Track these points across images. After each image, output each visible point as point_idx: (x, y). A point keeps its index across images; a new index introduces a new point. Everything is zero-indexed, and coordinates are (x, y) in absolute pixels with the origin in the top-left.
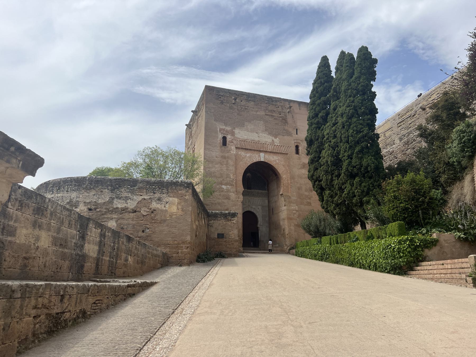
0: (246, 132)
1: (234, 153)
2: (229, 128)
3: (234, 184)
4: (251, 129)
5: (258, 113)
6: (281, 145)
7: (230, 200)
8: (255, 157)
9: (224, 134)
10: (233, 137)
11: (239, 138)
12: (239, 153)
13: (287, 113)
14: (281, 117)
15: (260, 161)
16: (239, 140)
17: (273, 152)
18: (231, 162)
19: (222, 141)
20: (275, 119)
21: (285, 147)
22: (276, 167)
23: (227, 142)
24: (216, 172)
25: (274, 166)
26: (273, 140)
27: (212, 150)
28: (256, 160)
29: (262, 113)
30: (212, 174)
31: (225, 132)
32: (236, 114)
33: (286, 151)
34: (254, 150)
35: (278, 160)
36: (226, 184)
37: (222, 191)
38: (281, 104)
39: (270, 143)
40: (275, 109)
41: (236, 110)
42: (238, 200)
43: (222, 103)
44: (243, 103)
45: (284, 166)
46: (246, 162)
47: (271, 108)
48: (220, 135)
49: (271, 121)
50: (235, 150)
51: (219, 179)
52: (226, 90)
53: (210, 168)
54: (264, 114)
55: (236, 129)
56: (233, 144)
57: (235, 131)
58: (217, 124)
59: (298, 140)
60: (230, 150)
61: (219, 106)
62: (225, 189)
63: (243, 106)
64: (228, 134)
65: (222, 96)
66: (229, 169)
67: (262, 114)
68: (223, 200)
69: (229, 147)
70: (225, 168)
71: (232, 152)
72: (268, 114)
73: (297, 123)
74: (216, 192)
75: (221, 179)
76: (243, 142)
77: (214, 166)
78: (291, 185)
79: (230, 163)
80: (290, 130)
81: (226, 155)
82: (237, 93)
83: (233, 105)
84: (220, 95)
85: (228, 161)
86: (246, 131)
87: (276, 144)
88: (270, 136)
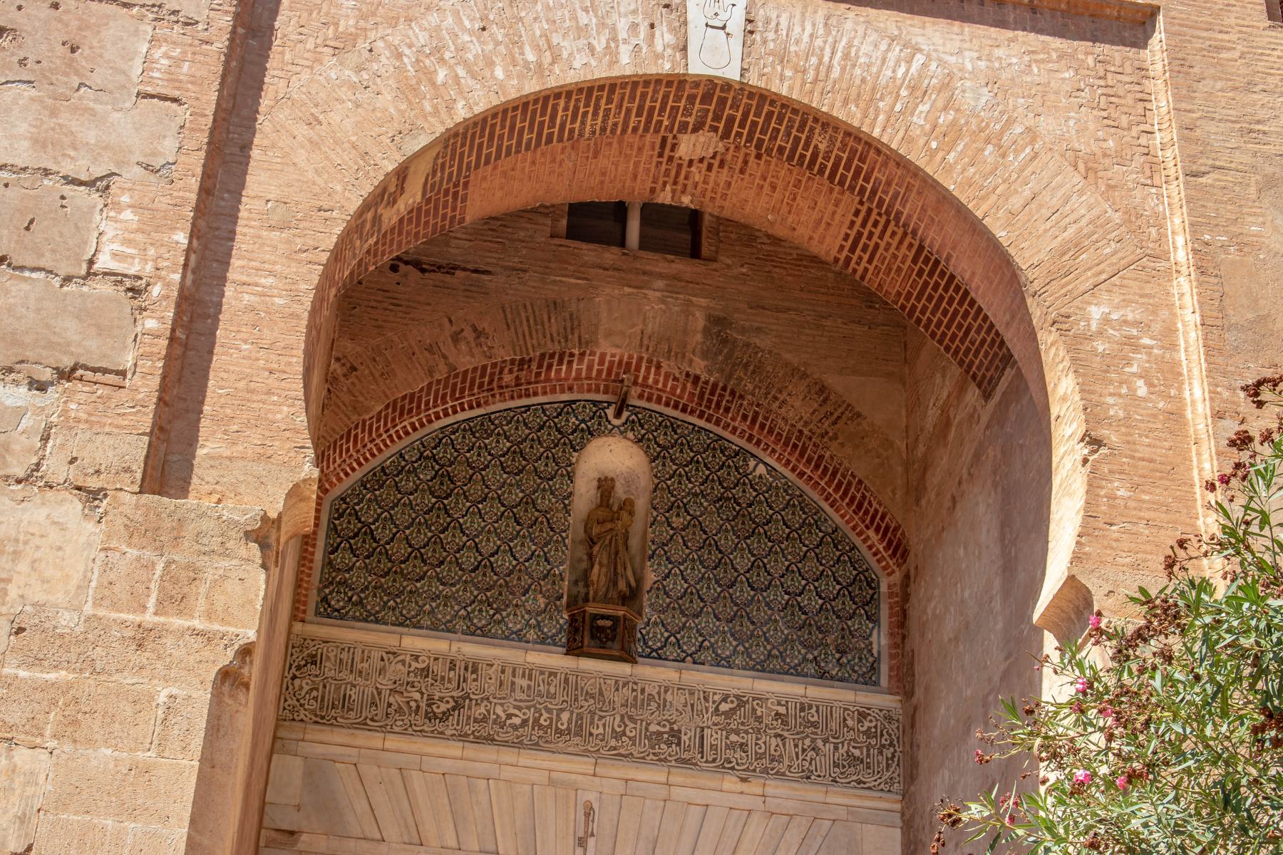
15: (666, 67)
25: (917, 157)
42: (143, 638)
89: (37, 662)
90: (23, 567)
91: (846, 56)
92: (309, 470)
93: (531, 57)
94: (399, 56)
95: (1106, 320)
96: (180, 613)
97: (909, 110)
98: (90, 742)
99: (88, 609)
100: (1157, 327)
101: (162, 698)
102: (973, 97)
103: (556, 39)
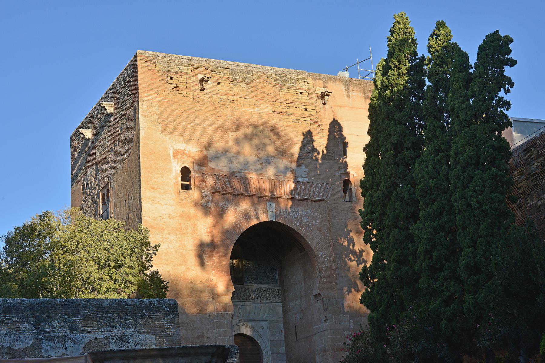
5: (257, 110)
25: (298, 231)
27: (160, 202)
32: (208, 114)
33: (323, 195)
35: (306, 216)
41: (208, 104)
44: (224, 87)
45: (319, 229)
58: (167, 138)
63: (222, 94)
65: (176, 73)
67: (266, 111)
77: (167, 238)
84: (170, 72)
85: (195, 225)
91: (288, 214)
97: (297, 223)
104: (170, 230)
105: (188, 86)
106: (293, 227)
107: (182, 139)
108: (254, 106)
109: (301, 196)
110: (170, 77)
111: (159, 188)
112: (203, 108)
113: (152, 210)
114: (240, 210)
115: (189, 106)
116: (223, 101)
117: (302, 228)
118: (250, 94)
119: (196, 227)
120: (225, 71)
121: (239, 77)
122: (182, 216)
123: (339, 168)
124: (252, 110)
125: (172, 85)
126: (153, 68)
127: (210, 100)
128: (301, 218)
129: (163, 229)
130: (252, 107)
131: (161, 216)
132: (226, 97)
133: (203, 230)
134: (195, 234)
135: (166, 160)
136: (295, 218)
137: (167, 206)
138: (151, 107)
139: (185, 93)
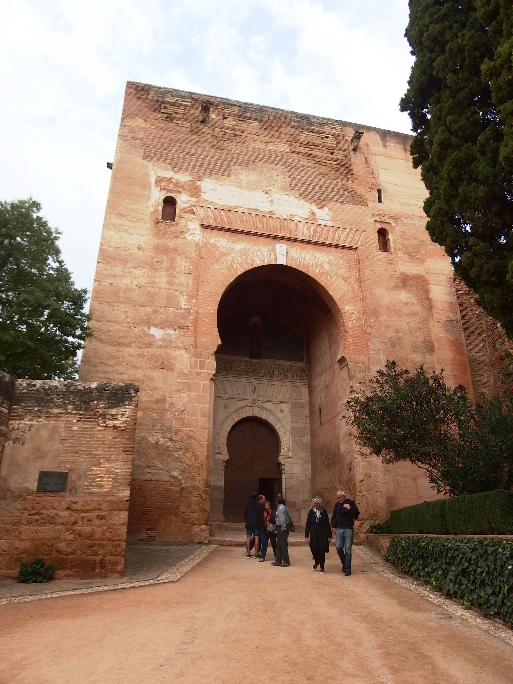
0: (234, 188)
1: (197, 238)
2: (184, 178)
3: (189, 324)
4: (250, 182)
5: (271, 147)
6: (336, 226)
7: (172, 370)
8: (259, 254)
9: (168, 191)
10: (195, 199)
11: (215, 203)
12: (212, 241)
13: (352, 152)
14: (334, 160)
15: (273, 263)
16: (212, 207)
17: (313, 243)
18: (182, 264)
19: (160, 208)
20: (317, 163)
21: (348, 230)
22: (323, 281)
23: (177, 211)
24: (133, 290)
25: (317, 279)
26: (313, 213)
27: (129, 230)
28: (264, 260)
29: (283, 147)
30: (121, 295)
31: (171, 186)
33: (351, 241)
34: (257, 235)
36: (162, 326)
37: (150, 345)
38: (334, 131)
39: (305, 219)
40: (319, 142)
41: (209, 136)
42: (198, 373)
43: (169, 118)
44: (229, 122)
45: (346, 280)
46: (232, 266)
47: (304, 137)
48: (158, 193)
49: (308, 167)
50: (198, 232)
51: (142, 309)
52: (182, 93)
53: (114, 276)
54: (288, 150)
55: (205, 180)
56: (192, 215)
57: (202, 186)
58: (150, 165)
59: (384, 215)
60: (182, 232)
61: (162, 125)
62: (158, 337)
63: (228, 128)
64: (180, 192)
65: (172, 104)
66: (177, 281)
67: (283, 149)
68: (149, 373)
69: (183, 222)
70: (164, 279)
71: (189, 237)
72: (298, 150)
73: (378, 175)
74: (126, 345)
75: (148, 310)
76: (222, 213)
77: (130, 272)
78: (370, 334)
79: (181, 265)
80: (362, 190)
81: (172, 244)
82: (213, 100)
83: (201, 126)
85: (173, 259)
86: (235, 186)
87: (323, 223)
88: (305, 203)
89: (182, 379)
90: (177, 362)
91: (304, 259)
92: (220, 342)
93: (250, 261)
94: (227, 262)
95: (349, 309)
96: (203, 369)
97: (315, 270)
98: (192, 392)
99: (188, 369)
100: (357, 310)
101: (202, 384)
102: (327, 267)
103: (254, 258)
104: (137, 263)
105: (186, 117)
106: (310, 274)
107: (169, 167)
108: (266, 144)
109: (322, 240)
110: (164, 107)
111: (130, 215)
112: (202, 139)
113: (116, 239)
114: (239, 249)
115: (184, 135)
116: (228, 135)
117: (322, 276)
118: (263, 132)
119: (175, 262)
120: (234, 108)
121: (251, 115)
122: (156, 248)
123: (373, 215)
124: (264, 147)
125: (165, 115)
126: (143, 97)
127: (211, 132)
128: (321, 265)
129: (126, 261)
130: (264, 144)
131: (128, 246)
132: (232, 132)
133: (183, 267)
134: (172, 271)
135: (146, 186)
136: (313, 265)
137: (137, 236)
138: (135, 132)
139: (181, 122)
